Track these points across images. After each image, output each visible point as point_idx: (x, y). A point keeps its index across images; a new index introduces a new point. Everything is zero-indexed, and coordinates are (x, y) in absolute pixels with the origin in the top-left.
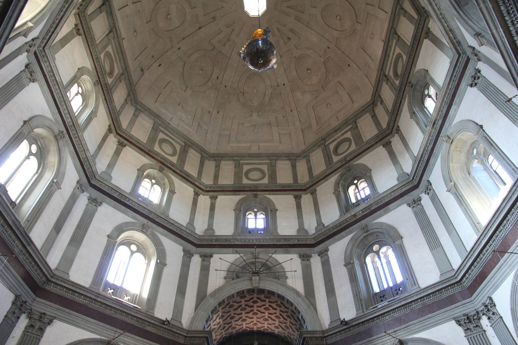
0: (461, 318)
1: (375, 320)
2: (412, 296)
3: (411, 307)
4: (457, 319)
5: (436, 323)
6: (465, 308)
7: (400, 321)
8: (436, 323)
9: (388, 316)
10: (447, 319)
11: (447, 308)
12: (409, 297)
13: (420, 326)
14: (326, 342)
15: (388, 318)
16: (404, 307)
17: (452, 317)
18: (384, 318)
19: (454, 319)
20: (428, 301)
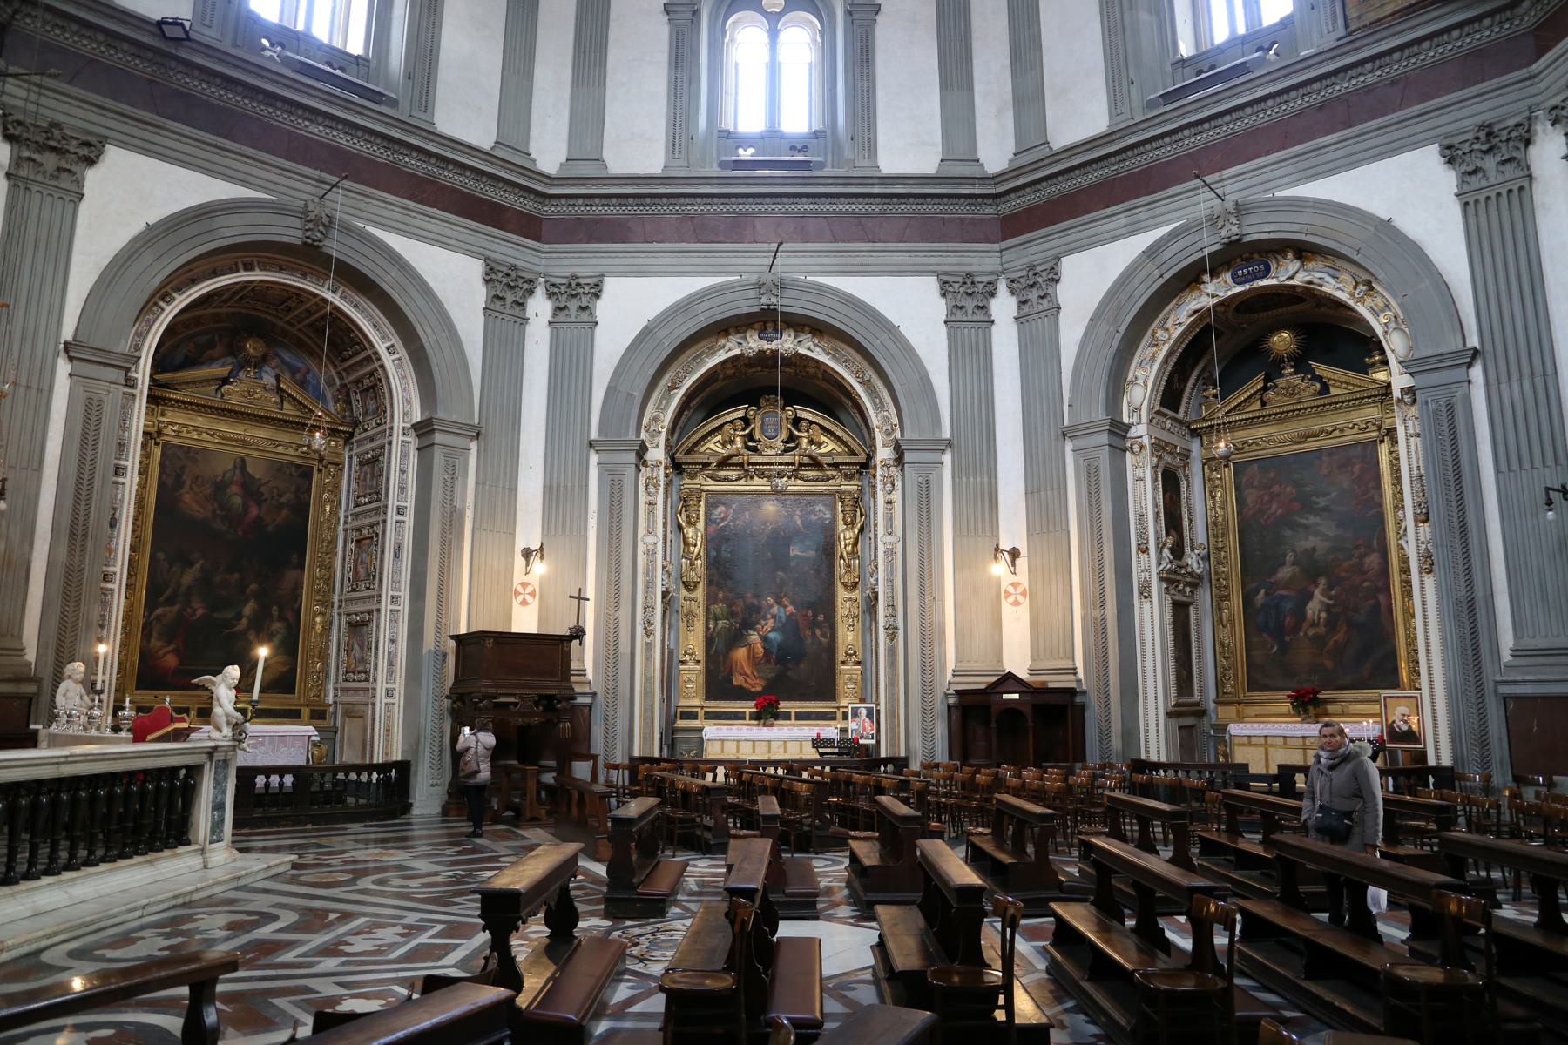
0: (501, 268)
1: (271, 106)
2: (431, 137)
3: (401, 158)
4: (493, 265)
5: (439, 238)
6: (517, 254)
7: (347, 166)
8: (439, 238)
9: (321, 128)
10: (469, 247)
11: (484, 226)
12: (424, 134)
13: (398, 217)
14: (12, 17)
15: (316, 131)
16: (385, 144)
17: (488, 253)
18: (307, 123)
19: (487, 259)
20: (449, 177)
